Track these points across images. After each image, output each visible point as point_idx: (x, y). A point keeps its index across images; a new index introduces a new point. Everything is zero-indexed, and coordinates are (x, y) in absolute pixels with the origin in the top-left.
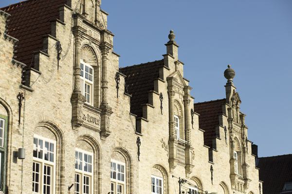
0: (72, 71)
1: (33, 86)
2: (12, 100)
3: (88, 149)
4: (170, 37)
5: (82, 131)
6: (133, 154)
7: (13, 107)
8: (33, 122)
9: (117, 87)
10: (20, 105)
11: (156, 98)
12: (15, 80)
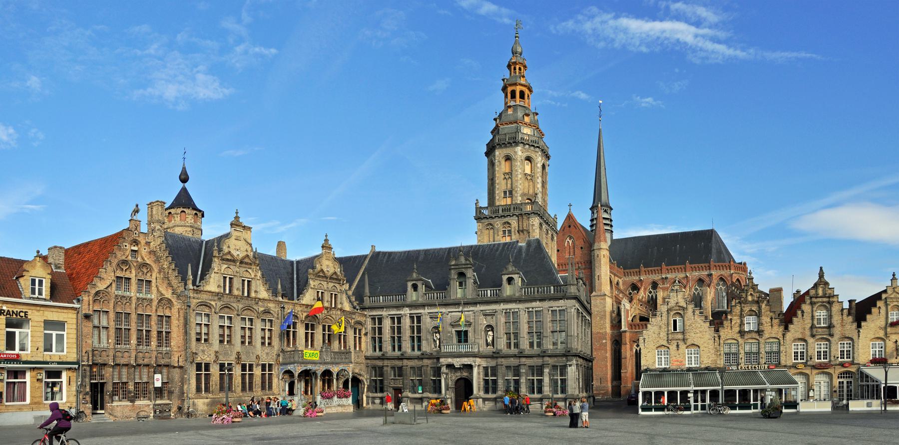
1: (790, 329)
2: (780, 336)
3: (825, 342)
4: (894, 275)
5: (818, 337)
6: (855, 337)
9: (842, 315)
10: (784, 337)
11: (874, 310)
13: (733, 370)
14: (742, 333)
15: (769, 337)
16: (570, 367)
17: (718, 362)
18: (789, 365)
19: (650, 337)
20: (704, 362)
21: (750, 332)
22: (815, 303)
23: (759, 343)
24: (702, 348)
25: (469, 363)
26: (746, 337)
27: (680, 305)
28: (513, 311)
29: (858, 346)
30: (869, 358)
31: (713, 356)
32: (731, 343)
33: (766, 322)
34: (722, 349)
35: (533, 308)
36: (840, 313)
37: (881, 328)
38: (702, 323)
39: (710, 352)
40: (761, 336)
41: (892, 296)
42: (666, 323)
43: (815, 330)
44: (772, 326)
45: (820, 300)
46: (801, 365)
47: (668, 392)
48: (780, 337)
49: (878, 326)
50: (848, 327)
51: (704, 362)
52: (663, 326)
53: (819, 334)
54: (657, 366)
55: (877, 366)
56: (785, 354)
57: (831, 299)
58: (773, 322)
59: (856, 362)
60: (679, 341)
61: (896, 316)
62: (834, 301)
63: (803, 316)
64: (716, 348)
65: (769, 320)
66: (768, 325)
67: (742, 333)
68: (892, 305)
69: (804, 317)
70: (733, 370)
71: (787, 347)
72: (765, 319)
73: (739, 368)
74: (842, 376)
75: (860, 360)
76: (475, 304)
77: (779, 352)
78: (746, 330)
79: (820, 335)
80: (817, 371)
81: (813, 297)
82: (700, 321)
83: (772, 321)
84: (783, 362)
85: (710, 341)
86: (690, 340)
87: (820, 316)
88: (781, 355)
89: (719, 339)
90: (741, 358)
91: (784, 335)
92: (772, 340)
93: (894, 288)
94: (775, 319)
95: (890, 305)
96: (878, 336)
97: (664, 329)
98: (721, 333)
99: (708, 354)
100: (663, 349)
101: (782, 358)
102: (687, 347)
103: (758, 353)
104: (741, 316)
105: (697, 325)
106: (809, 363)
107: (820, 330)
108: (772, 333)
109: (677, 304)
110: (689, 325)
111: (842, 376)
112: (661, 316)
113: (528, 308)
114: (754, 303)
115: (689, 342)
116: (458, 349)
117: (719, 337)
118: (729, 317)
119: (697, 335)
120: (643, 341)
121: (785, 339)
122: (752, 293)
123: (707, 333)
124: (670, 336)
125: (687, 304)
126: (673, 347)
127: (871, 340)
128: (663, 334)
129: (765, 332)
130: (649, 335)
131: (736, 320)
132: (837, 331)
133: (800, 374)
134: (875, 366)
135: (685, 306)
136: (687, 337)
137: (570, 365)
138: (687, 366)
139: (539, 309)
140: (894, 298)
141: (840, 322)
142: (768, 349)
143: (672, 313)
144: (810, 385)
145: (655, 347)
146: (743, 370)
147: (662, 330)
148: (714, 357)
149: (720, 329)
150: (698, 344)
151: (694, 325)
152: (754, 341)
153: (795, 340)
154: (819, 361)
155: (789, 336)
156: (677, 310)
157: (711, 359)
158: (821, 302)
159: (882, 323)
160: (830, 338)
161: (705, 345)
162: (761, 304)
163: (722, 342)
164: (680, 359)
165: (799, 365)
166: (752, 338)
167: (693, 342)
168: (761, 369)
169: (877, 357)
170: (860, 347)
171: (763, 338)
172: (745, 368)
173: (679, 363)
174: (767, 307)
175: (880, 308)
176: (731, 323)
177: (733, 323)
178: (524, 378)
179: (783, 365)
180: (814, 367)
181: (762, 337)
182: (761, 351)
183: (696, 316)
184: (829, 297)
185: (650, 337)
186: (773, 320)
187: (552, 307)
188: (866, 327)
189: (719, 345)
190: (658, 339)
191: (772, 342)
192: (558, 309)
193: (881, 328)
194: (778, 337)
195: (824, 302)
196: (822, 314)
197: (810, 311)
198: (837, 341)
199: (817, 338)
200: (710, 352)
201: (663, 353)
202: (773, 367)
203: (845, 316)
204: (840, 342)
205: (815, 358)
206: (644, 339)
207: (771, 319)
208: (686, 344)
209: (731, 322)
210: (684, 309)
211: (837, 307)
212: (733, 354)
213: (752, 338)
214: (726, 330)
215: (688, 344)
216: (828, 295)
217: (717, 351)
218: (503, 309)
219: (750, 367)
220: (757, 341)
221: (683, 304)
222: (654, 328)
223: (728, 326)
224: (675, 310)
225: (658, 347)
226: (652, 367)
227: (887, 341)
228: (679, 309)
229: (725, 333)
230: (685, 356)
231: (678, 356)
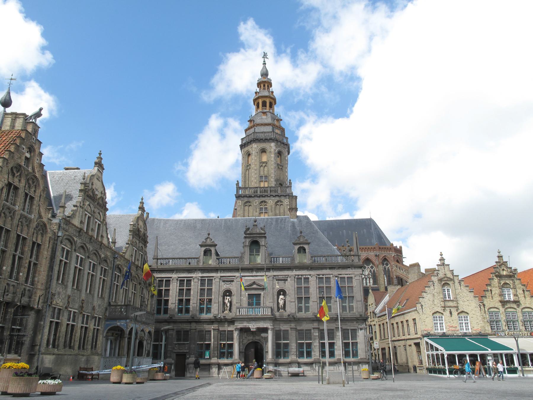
13: (502, 336)
14: (504, 303)
15: (524, 307)
16: (361, 331)
17: (487, 328)
21: (509, 302)
23: (516, 312)
25: (265, 326)
26: (506, 307)
28: (304, 277)
32: (493, 311)
35: (323, 275)
39: (478, 319)
52: (435, 294)
58: (525, 294)
60: (451, 308)
64: (482, 315)
65: (521, 292)
67: (504, 303)
73: (506, 334)
76: (268, 269)
82: (465, 291)
83: (524, 292)
85: (476, 309)
89: (484, 307)
98: (485, 303)
99: (478, 321)
100: (438, 315)
105: (464, 294)
112: (434, 286)
113: (318, 275)
116: (254, 312)
117: (484, 305)
122: (504, 268)
126: (447, 313)
135: (452, 277)
137: (361, 329)
139: (329, 276)
145: (431, 314)
147: (436, 297)
148: (482, 324)
150: (467, 311)
151: (461, 294)
152: (512, 310)
156: (446, 281)
157: (480, 326)
161: (473, 312)
163: (486, 310)
164: (454, 325)
168: (525, 336)
172: (511, 334)
173: (454, 329)
177: (493, 293)
178: (317, 341)
181: (519, 307)
183: (462, 286)
186: (525, 292)
187: (341, 275)
189: (485, 313)
190: (433, 306)
192: (346, 276)
200: (478, 319)
206: (422, 306)
207: (523, 291)
208: (457, 311)
209: (491, 292)
214: (488, 300)
215: (459, 311)
217: (484, 318)
218: (295, 275)
224: (444, 281)
225: (433, 314)
226: (432, 332)
228: (448, 280)
229: (489, 303)
231: (452, 322)
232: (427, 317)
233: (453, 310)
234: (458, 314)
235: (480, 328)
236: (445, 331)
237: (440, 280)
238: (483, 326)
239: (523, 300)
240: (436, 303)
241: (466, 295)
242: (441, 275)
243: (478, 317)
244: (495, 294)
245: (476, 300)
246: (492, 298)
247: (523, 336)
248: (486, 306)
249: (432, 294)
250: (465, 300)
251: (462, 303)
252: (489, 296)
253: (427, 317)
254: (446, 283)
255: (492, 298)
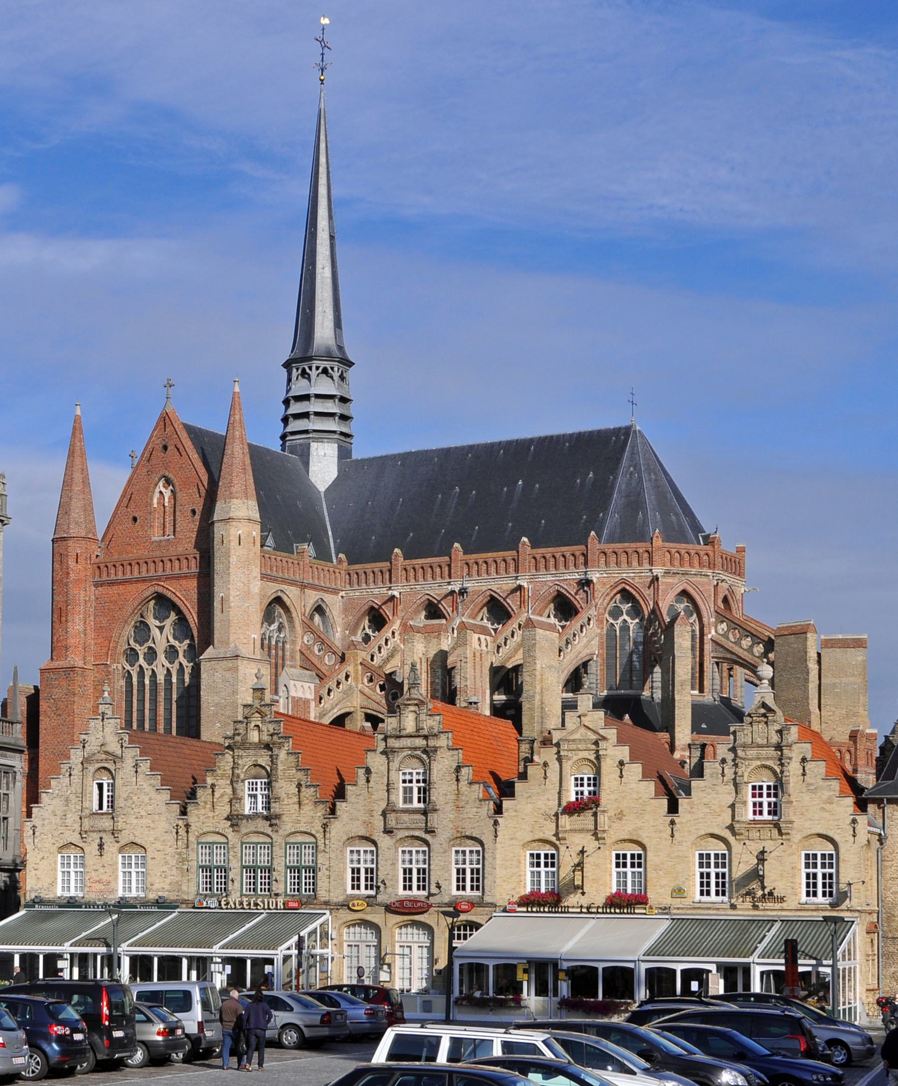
0: (386, 788)
2: (317, 828)
6: (487, 838)
7: (317, 835)
8: (340, 841)
9: (458, 780)
10: (325, 832)
12: (319, 814)
13: (209, 908)
14: (235, 819)
15: (293, 830)
17: (184, 888)
18: (335, 900)
19: (45, 822)
20: (154, 887)
21: (254, 816)
22: (393, 751)
24: (150, 854)
26: (244, 830)
27: (108, 749)
29: (494, 859)
30: (517, 890)
31: (174, 872)
32: (213, 843)
33: (288, 794)
34: (193, 856)
36: (454, 775)
37: (546, 816)
38: (153, 794)
39: (166, 863)
40: (275, 828)
41: (577, 736)
42: (80, 791)
43: (391, 817)
44: (300, 803)
45: (408, 742)
46: (360, 902)
47: (44, 956)
48: (317, 832)
49: (541, 811)
50: (471, 810)
51: (154, 887)
52: (72, 797)
53: (404, 826)
54: (59, 893)
55: (532, 912)
56: (327, 873)
57: (432, 743)
58: (302, 795)
59: (487, 899)
60: (103, 835)
61: (589, 785)
62: (440, 747)
63: (368, 781)
64: (180, 854)
66: (291, 801)
67: (235, 819)
68: (575, 758)
69: (371, 784)
70: (209, 908)
71: (333, 855)
72: (285, 788)
73: (223, 903)
74: (462, 932)
75: (498, 897)
77: (314, 870)
78: (247, 812)
79: (407, 829)
80: (399, 918)
81: (391, 737)
84: (322, 895)
86: (126, 832)
87: (411, 781)
88: (319, 874)
89: (187, 832)
90: (233, 881)
91: (325, 826)
92: (300, 838)
93: (579, 717)
94: (307, 787)
95: (569, 759)
96: (540, 835)
97: (75, 806)
99: (165, 868)
100: (73, 853)
101: (320, 883)
102: (121, 850)
103: (270, 870)
104: (234, 780)
106: (381, 898)
107: (406, 817)
108: (299, 822)
109: (104, 748)
110: (125, 796)
111: (462, 932)
112: (70, 775)
114: (261, 748)
115: (124, 838)
117: (187, 826)
118: (209, 780)
119: (141, 821)
120: (31, 832)
121: (327, 836)
123: (163, 818)
124: (86, 822)
125: (122, 747)
126: (92, 848)
127: (525, 845)
128: (72, 818)
129: (284, 818)
130: (44, 819)
131: (224, 788)
132: (443, 821)
133: (359, 925)
134: (528, 912)
135: (119, 752)
136: (120, 825)
138: (120, 893)
140: (580, 740)
141: (454, 797)
142: (292, 860)
143: (92, 768)
144: (383, 954)
145: (55, 848)
146: (231, 909)
147: (72, 806)
148: (174, 875)
149: (190, 808)
151: (135, 798)
153: (351, 839)
154: (408, 892)
155: (338, 829)
157: (168, 881)
158: (410, 748)
159: (550, 803)
160: (427, 837)
161: (159, 845)
162: (276, 751)
163: (192, 838)
164: (105, 878)
165: (356, 902)
166: (258, 832)
167: (132, 839)
169: (543, 891)
170: (498, 862)
171: (281, 832)
172: (235, 904)
174: (292, 758)
175: (545, 764)
176: (213, 795)
177: (217, 795)
179: (323, 899)
180: (389, 909)
181: (277, 831)
182: (275, 862)
183: (141, 777)
184: (426, 737)
185: (45, 822)
186: (303, 789)
188: (514, 814)
189: (188, 847)
191: (301, 843)
193: (546, 816)
194: (313, 832)
195: (415, 749)
196: (415, 778)
197: (384, 768)
198: (445, 845)
199: (399, 837)
200: (166, 863)
201: (72, 862)
202: (296, 905)
203: (463, 783)
204: (454, 849)
205: (395, 887)
207: (299, 786)
208: (118, 842)
209: (213, 791)
210: (116, 759)
211: (447, 762)
212: (219, 868)
213: (258, 832)
214: (203, 811)
215: (122, 843)
216: (425, 732)
219: (245, 903)
220: (269, 840)
221: (114, 747)
222: (54, 802)
223: (205, 803)
224: (98, 761)
226: (47, 895)
227: (562, 849)
230: (115, 871)
231: (102, 870)
232: (43, 858)
233: (108, 839)
234: (121, 850)
235: (167, 887)
236: (73, 893)
237: (85, 762)
238: (177, 882)
239: (293, 811)
240: (69, 821)
241: (146, 800)
242: (93, 746)
243: (168, 858)
244: (222, 796)
245: (169, 812)
246: (213, 806)
247: (264, 909)
248: (193, 828)
249: (63, 798)
250: (144, 814)
251: (135, 821)
252: (205, 803)
253: (43, 858)
254: (104, 768)
255: (213, 806)
